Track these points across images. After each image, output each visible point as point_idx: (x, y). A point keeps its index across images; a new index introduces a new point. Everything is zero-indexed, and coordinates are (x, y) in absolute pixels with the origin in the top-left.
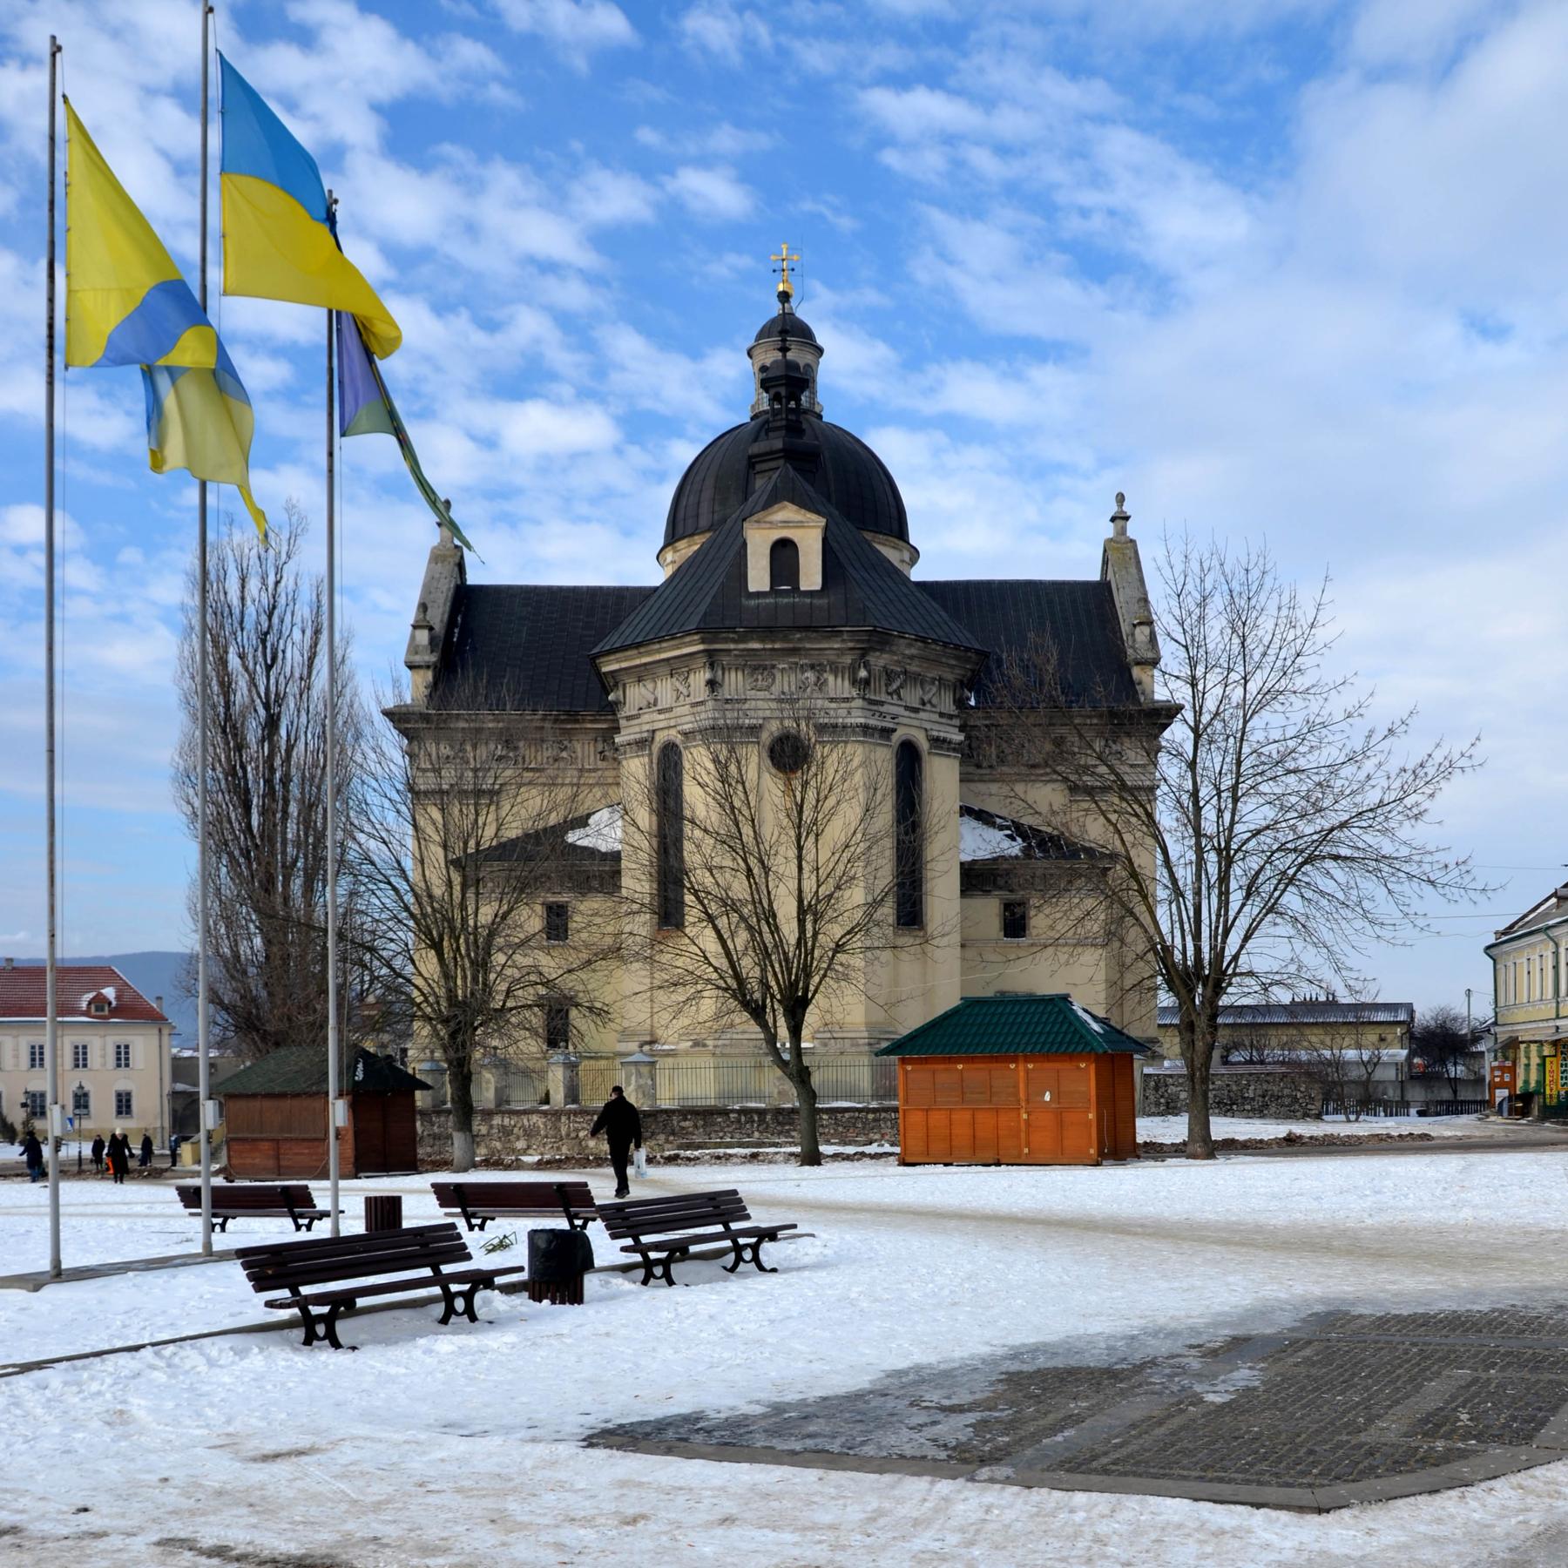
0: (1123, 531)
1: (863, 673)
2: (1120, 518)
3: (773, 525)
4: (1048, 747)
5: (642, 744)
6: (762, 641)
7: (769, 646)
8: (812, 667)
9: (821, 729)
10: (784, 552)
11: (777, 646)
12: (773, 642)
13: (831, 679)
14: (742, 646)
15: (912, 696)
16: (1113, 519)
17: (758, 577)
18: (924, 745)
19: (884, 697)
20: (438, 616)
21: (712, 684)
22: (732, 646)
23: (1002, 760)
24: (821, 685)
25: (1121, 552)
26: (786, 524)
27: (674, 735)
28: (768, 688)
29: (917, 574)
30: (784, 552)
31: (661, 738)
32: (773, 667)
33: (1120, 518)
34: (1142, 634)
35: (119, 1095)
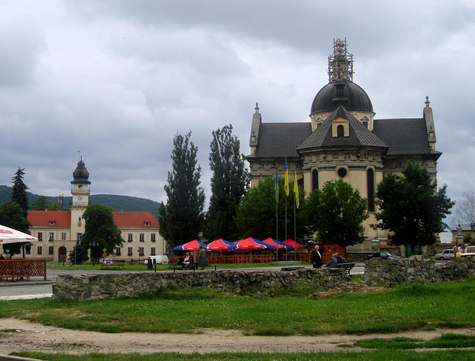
0: (428, 106)
1: (359, 155)
2: (427, 103)
3: (338, 122)
5: (309, 169)
8: (347, 154)
9: (349, 167)
10: (340, 128)
15: (371, 158)
17: (335, 134)
18: (374, 169)
19: (364, 159)
20: (257, 134)
21: (324, 158)
23: (396, 167)
24: (349, 157)
25: (427, 111)
26: (341, 122)
27: (316, 168)
29: (375, 118)
30: (340, 128)
31: (313, 168)
33: (427, 103)
34: (431, 135)
35: (152, 249)
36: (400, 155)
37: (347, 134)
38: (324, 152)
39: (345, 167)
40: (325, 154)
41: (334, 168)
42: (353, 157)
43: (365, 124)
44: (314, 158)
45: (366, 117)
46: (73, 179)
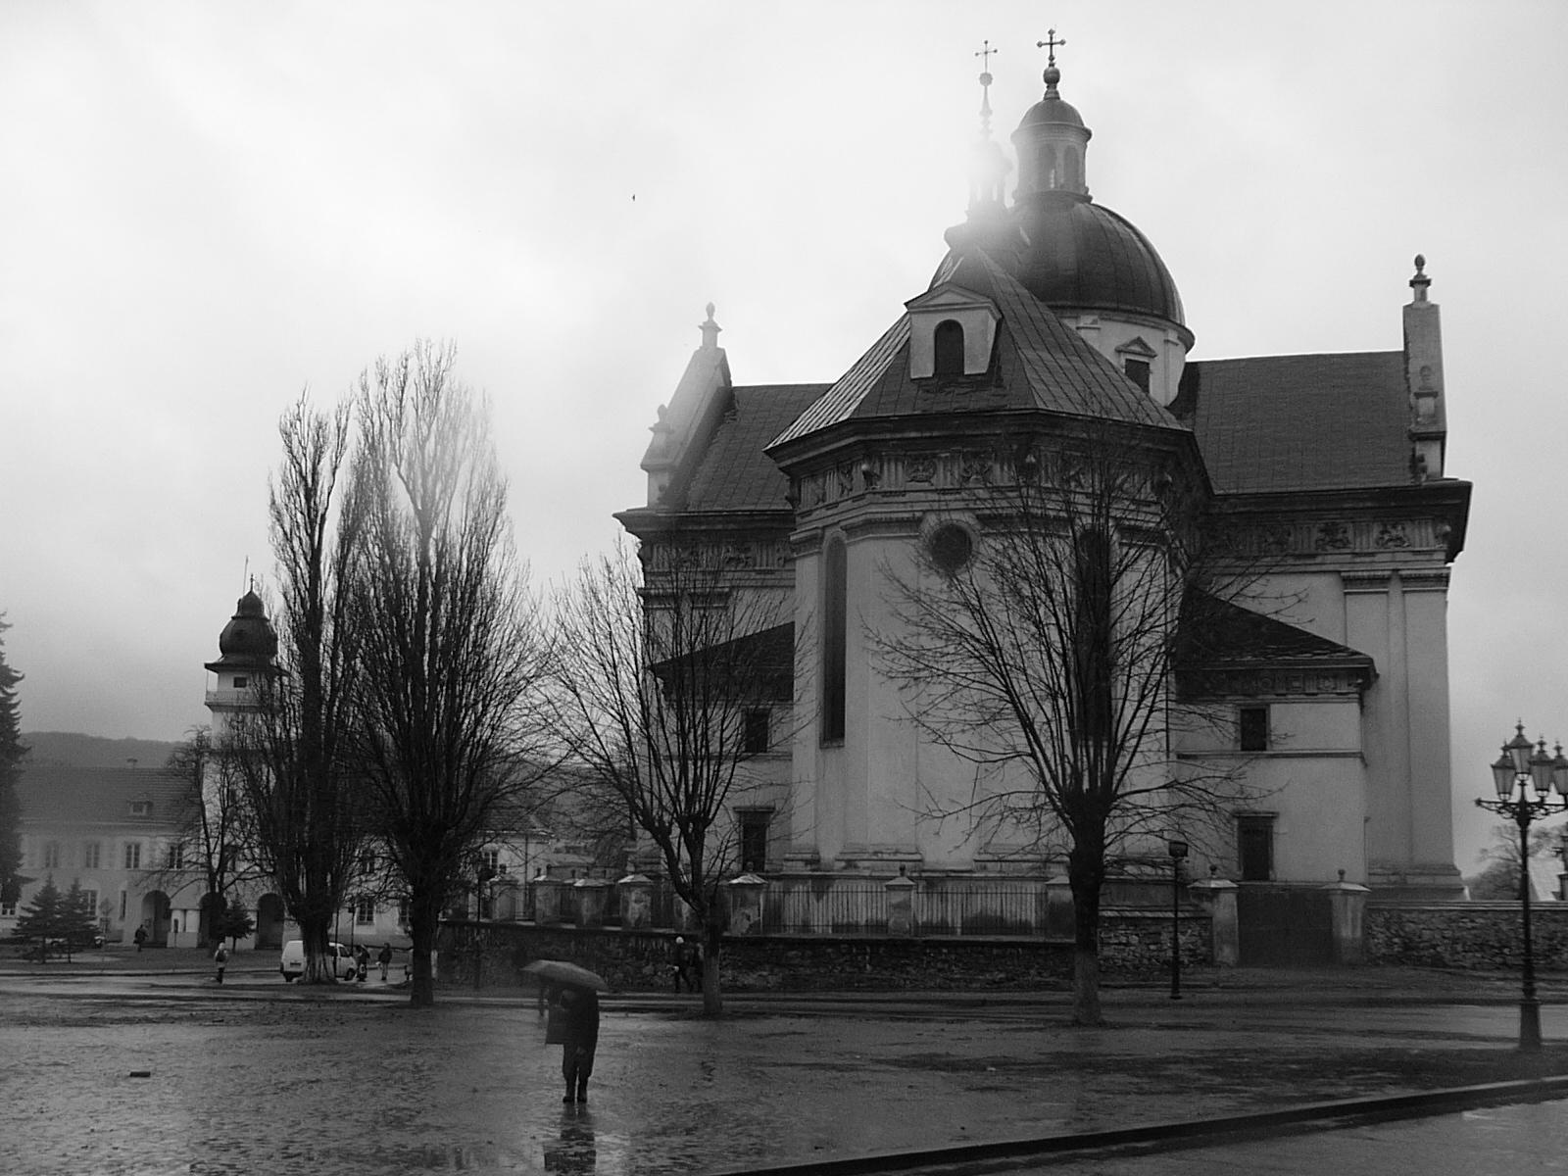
0: (1422, 296)
2: (1420, 283)
4: (1316, 535)
5: (814, 540)
6: (917, 431)
7: (928, 434)
8: (976, 455)
11: (935, 434)
12: (931, 429)
13: (997, 467)
14: (899, 436)
16: (1412, 284)
22: (888, 436)
24: (985, 474)
25: (1421, 319)
28: (927, 480)
32: (934, 456)
33: (1420, 283)
36: (1278, 497)
37: (976, 364)
38: (869, 450)
39: (966, 519)
40: (868, 457)
41: (915, 523)
42: (1002, 475)
43: (1138, 372)
44: (832, 485)
45: (1139, 341)
46: (216, 656)
